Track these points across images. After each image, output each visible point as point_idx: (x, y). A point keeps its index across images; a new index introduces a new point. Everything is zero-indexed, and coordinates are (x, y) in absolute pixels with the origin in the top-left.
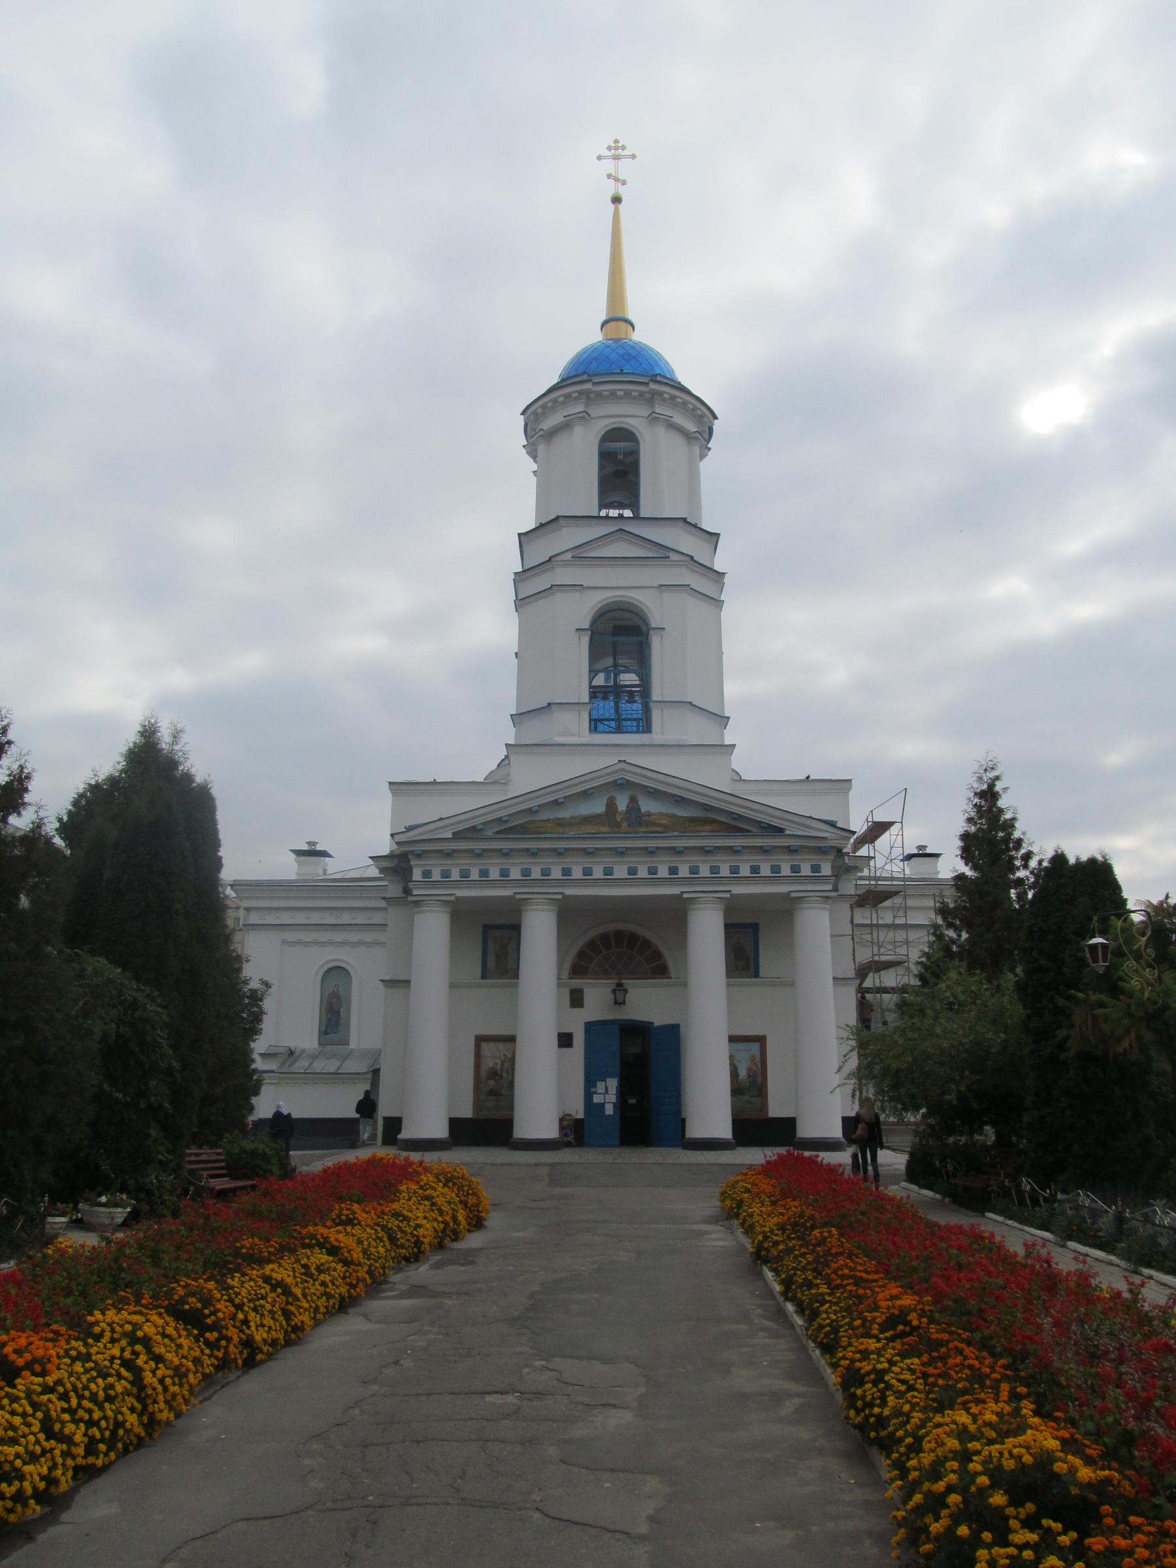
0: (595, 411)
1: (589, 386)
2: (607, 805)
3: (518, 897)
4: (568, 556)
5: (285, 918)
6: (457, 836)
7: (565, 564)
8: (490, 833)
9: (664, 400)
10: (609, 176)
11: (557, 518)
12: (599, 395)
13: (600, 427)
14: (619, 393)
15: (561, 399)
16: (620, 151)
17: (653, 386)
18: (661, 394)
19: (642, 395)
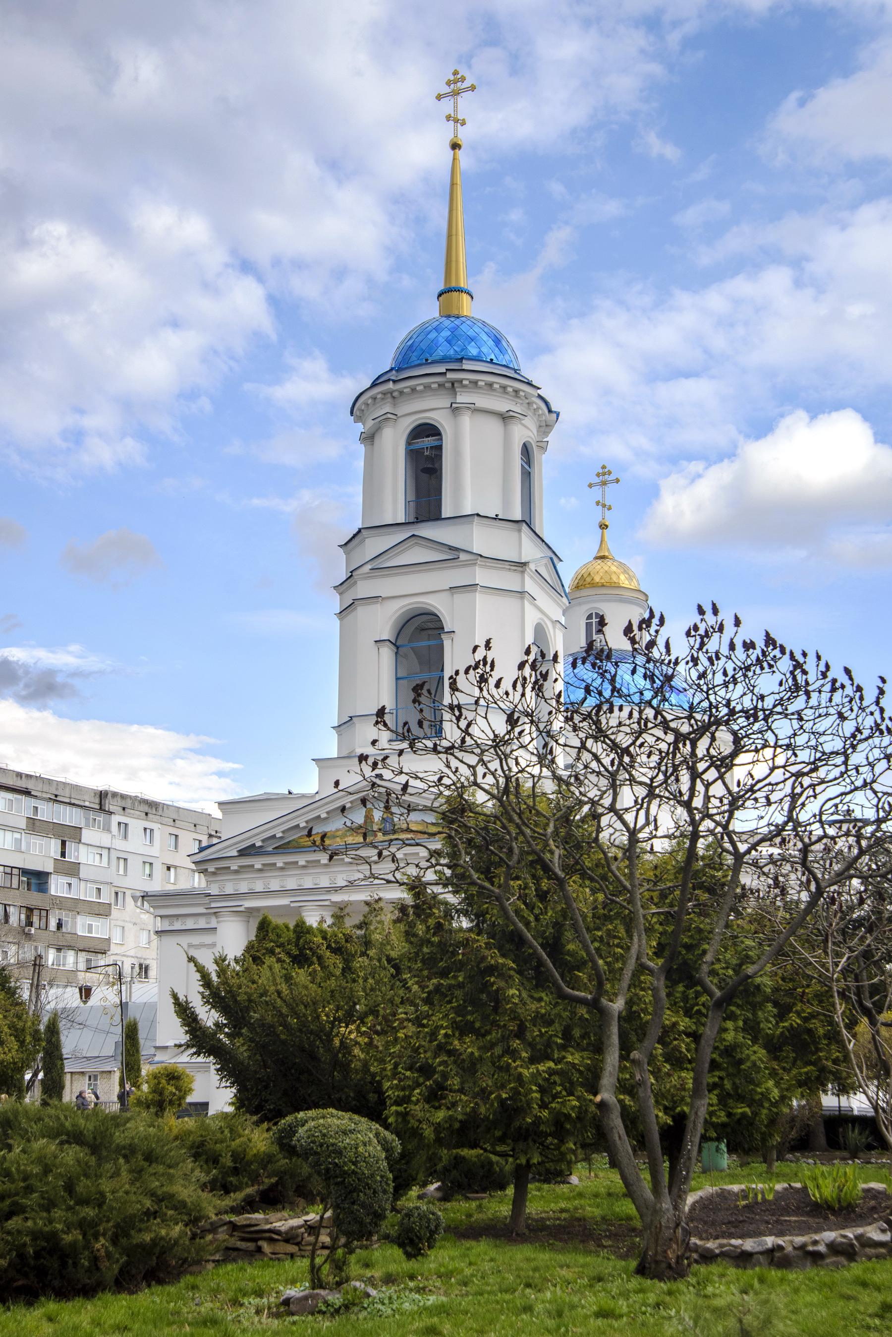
0: (402, 409)
1: (391, 385)
2: (366, 817)
3: (292, 905)
4: (369, 567)
5: (190, 924)
6: (243, 853)
7: (367, 577)
8: (270, 849)
9: (465, 386)
10: (448, 118)
11: (360, 531)
12: (401, 393)
13: (406, 425)
14: (418, 388)
15: (379, 396)
16: (459, 84)
17: (450, 375)
18: (461, 381)
19: (441, 385)
